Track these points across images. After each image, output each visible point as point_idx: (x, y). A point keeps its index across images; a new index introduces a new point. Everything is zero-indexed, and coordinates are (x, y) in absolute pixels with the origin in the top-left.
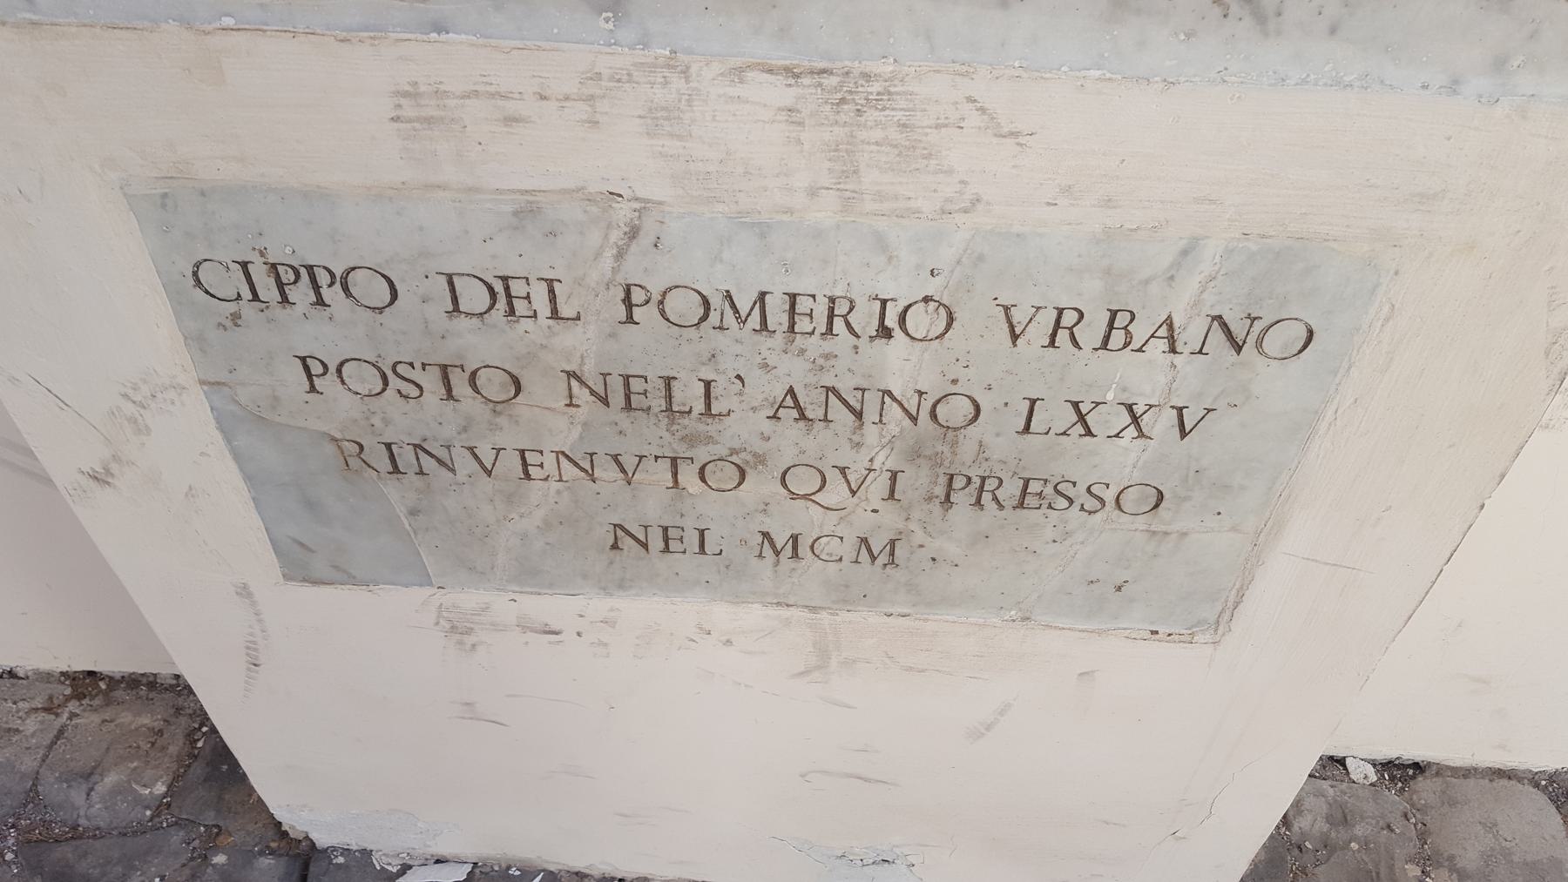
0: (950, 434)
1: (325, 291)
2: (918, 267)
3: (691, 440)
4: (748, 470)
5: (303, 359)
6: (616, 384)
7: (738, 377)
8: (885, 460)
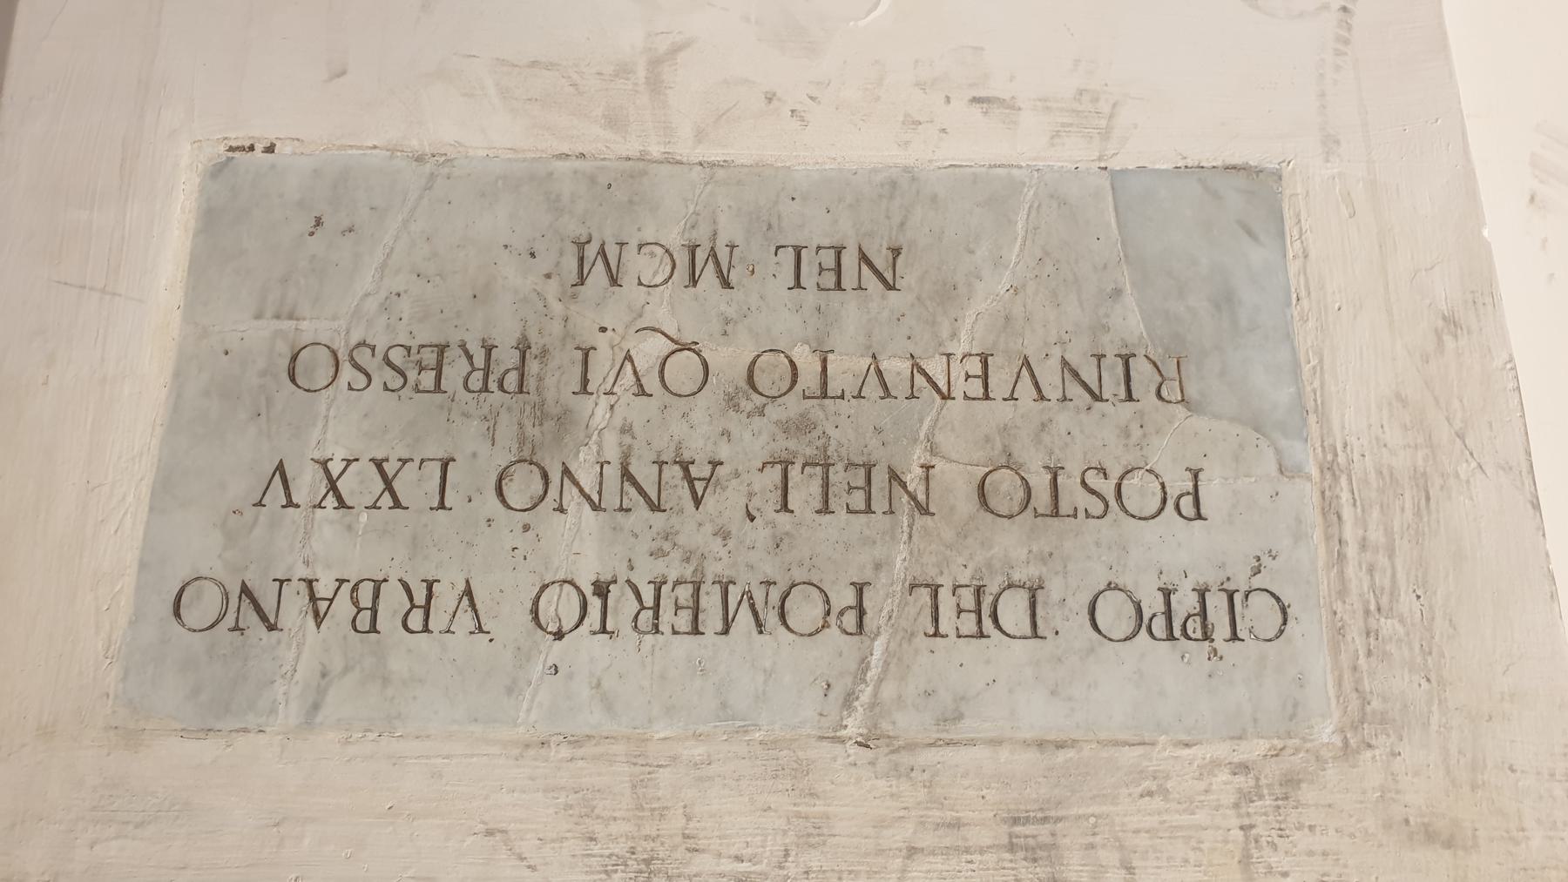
0: (526, 454)
2: (570, 676)
3: (803, 426)
4: (743, 384)
5: (1199, 516)
6: (879, 504)
8: (598, 411)
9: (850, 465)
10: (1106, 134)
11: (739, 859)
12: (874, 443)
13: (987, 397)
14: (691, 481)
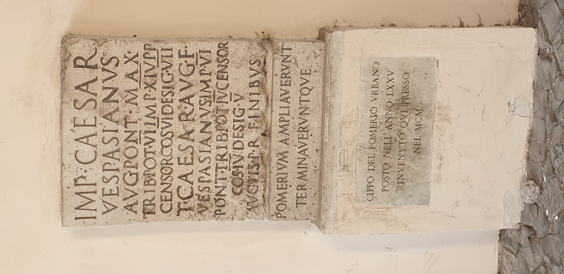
0: (393, 105)
1: (371, 185)
2: (365, 112)
3: (396, 140)
4: (402, 132)
6: (385, 150)
7: (384, 134)
9: (390, 147)
10: (435, 182)
11: (344, 134)
12: (393, 150)
13: (399, 165)
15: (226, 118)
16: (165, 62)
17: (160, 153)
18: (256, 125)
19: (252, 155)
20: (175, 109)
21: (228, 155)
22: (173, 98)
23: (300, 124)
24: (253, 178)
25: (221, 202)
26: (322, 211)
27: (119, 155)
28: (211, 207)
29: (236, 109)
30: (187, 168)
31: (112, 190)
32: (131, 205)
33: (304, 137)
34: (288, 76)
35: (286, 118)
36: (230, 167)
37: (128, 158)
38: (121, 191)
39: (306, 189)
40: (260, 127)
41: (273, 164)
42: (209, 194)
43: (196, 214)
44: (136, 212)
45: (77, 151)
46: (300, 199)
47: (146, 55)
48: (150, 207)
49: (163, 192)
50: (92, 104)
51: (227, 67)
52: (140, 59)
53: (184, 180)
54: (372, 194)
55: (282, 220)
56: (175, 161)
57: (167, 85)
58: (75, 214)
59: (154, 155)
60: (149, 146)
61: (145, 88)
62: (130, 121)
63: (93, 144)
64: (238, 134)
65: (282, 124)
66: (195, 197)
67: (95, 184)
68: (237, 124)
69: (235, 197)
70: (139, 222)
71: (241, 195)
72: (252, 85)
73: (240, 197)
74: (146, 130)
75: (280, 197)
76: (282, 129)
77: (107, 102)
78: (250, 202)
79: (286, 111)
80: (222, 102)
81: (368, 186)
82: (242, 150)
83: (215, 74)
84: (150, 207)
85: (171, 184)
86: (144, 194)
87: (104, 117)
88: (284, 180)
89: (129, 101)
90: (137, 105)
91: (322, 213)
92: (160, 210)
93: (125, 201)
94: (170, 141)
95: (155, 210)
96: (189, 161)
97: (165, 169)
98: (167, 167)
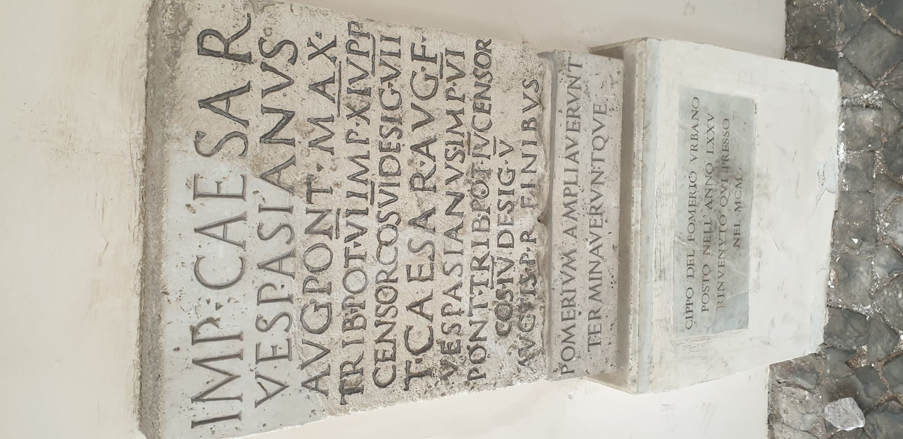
3: (716, 227)
9: (710, 237)
14: (709, 204)
15: (487, 187)
16: (386, 65)
17: (375, 256)
18: (534, 201)
19: (525, 258)
20: (405, 167)
21: (489, 258)
22: (401, 141)
23: (592, 201)
24: (528, 301)
25: (479, 353)
26: (630, 353)
27: (293, 265)
28: (463, 364)
29: (502, 169)
30: (423, 288)
31: (276, 346)
32: (316, 377)
33: (597, 225)
34: (576, 114)
35: (574, 189)
36: (493, 283)
37: (312, 272)
38: (296, 348)
39: (599, 318)
40: (537, 205)
41: (556, 273)
42: (459, 338)
43: (438, 381)
44: (325, 393)
45: (200, 257)
46: (592, 336)
47: (352, 45)
48: (353, 378)
49: (378, 341)
50: (236, 145)
51: (489, 87)
52: (339, 52)
53: (417, 313)
54: (691, 317)
55: (569, 377)
56: (401, 274)
57: (389, 114)
58: (192, 413)
59: (363, 263)
60: (354, 243)
61: (349, 116)
62: (319, 187)
63: (237, 241)
64: (506, 217)
65: (569, 199)
66: (436, 347)
67: (239, 337)
68: (504, 198)
69: (500, 341)
70: (332, 414)
71: (509, 337)
72: (526, 125)
73: (509, 340)
74: (349, 209)
75: (564, 336)
76: (568, 210)
77: (270, 142)
78: (522, 349)
79: (571, 177)
80: (482, 156)
81: (687, 304)
82: (511, 249)
83: (470, 100)
84: (353, 378)
85: (394, 324)
86: (341, 349)
87: (263, 177)
88: (571, 303)
89: (318, 143)
90: (333, 154)
91: (630, 357)
92: (373, 383)
93: (304, 370)
94: (393, 232)
95: (363, 383)
96: (426, 273)
97: (383, 292)
98: (387, 287)
